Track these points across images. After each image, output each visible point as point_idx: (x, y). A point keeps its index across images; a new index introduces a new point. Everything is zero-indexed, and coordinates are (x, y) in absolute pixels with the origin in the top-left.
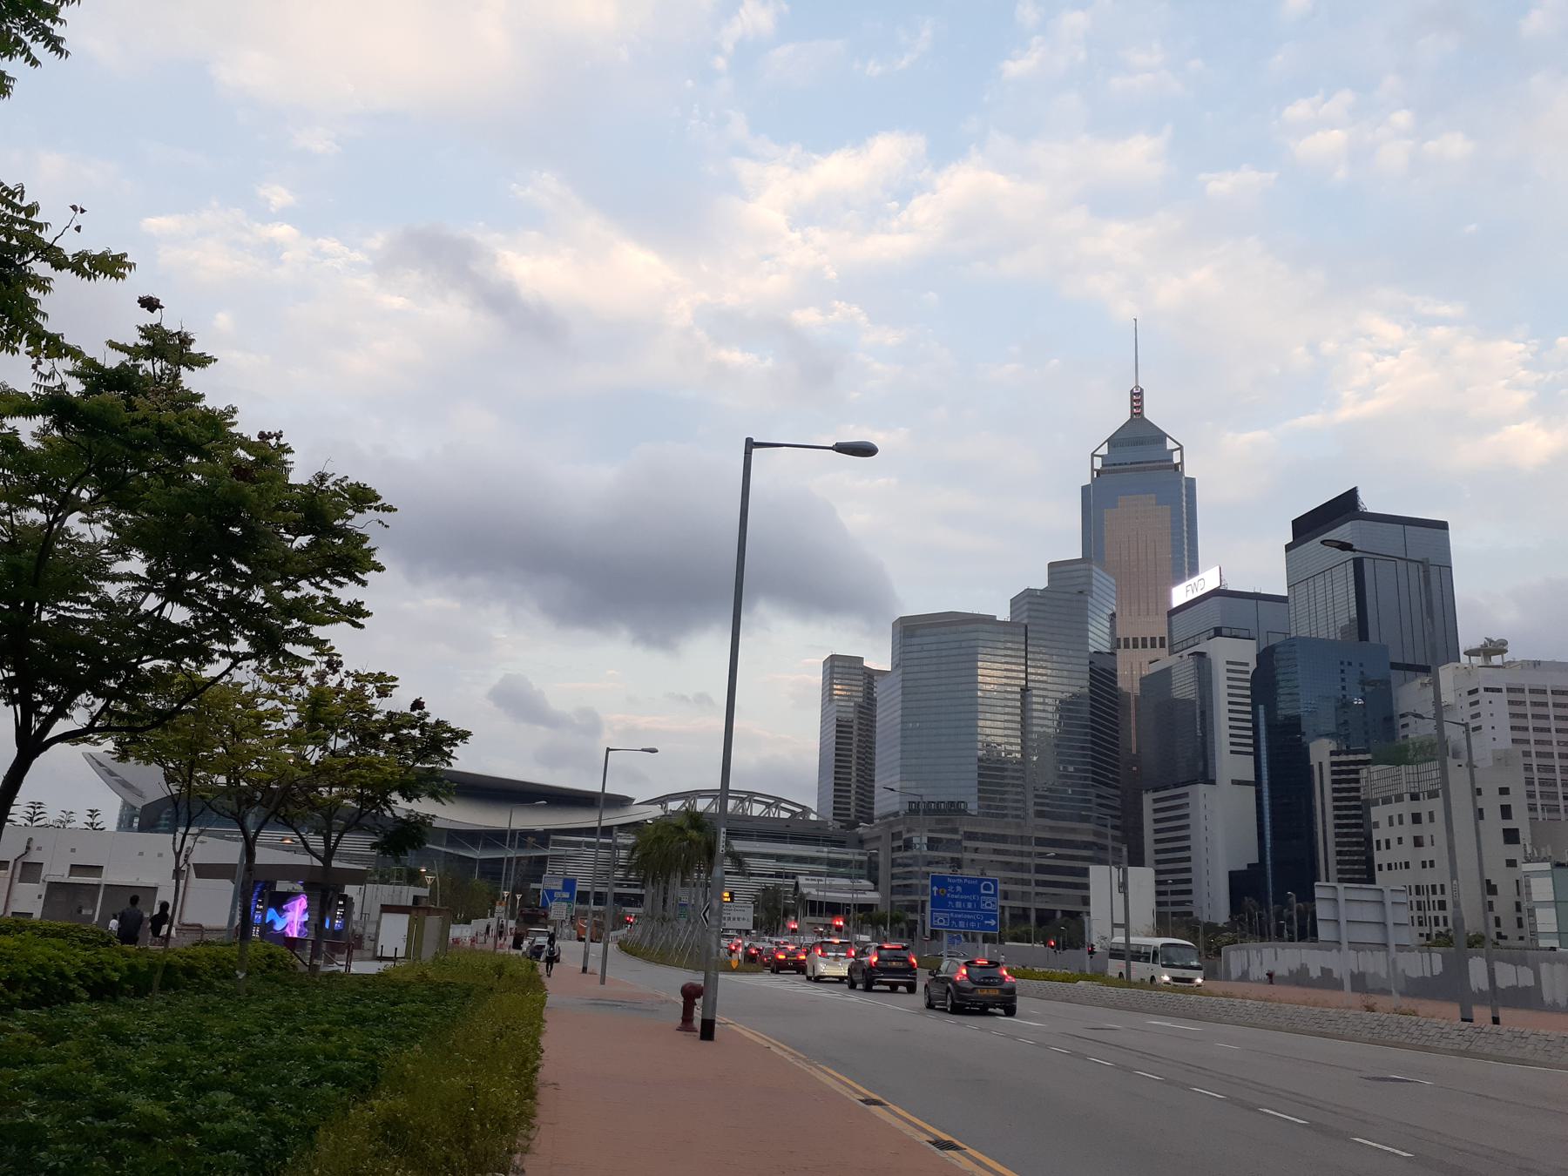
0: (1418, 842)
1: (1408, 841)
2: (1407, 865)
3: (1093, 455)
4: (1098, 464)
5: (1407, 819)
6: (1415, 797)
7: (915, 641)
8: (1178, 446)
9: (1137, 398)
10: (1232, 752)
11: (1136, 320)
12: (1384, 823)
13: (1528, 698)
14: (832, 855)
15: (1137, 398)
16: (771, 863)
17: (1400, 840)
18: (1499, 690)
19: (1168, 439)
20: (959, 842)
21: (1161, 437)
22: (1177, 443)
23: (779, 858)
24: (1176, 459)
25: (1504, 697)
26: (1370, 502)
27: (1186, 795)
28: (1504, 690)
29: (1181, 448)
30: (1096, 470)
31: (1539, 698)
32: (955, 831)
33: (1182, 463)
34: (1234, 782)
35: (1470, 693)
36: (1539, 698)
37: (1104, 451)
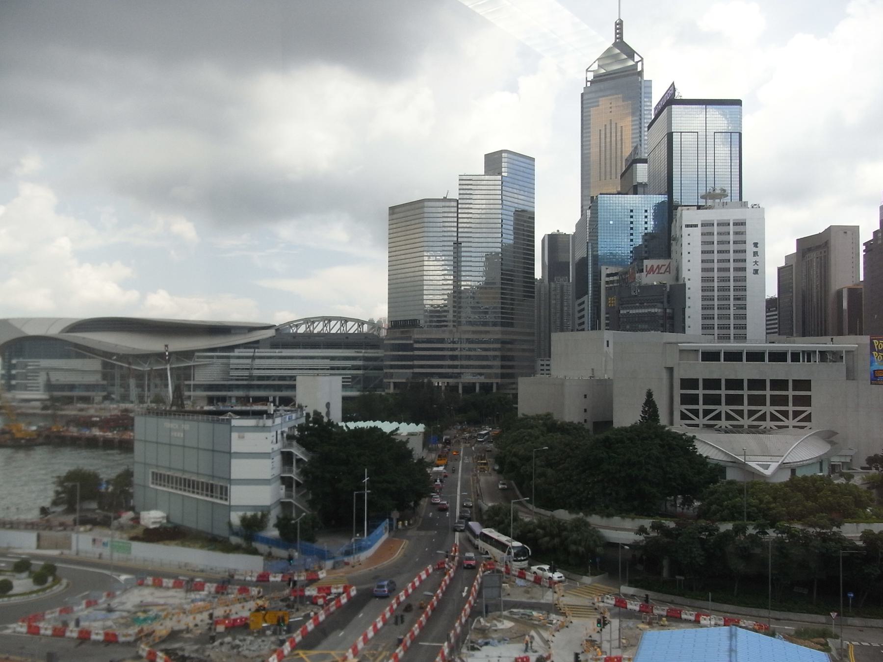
3: (587, 71)
8: (640, 59)
14: (366, 355)
16: (327, 362)
18: (696, 226)
19: (635, 54)
23: (333, 358)
25: (698, 231)
26: (683, 93)
28: (700, 226)
29: (642, 60)
30: (589, 81)
32: (409, 338)
36: (724, 229)
37: (595, 67)
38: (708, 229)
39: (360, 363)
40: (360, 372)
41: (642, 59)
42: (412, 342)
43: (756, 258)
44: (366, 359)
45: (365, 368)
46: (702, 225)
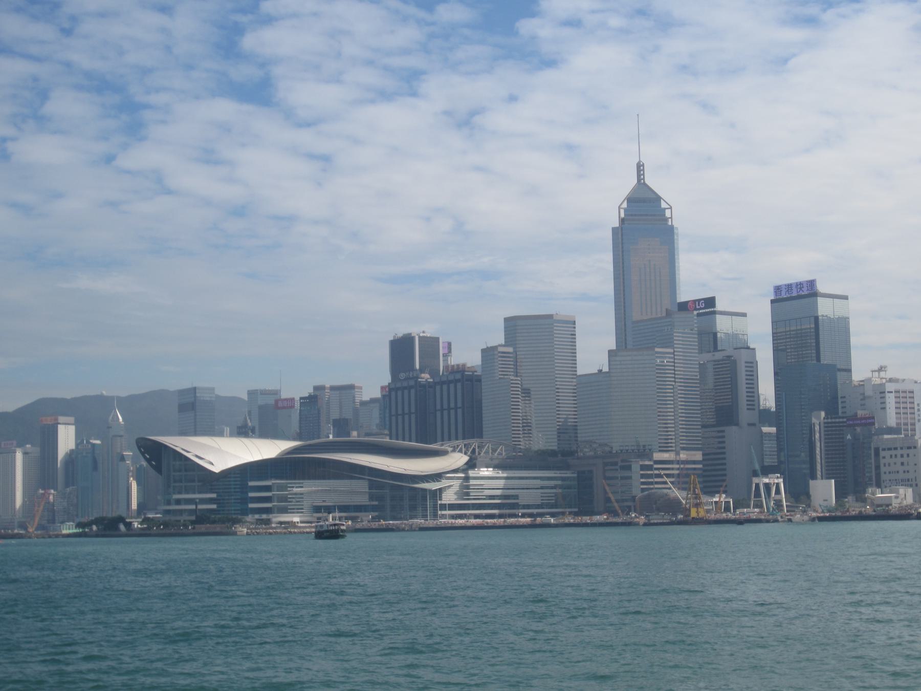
0: (902, 464)
1: (899, 464)
2: (898, 472)
3: (619, 208)
4: (622, 215)
5: (899, 456)
6: (902, 448)
7: (618, 358)
9: (640, 168)
10: (748, 409)
11: (638, 115)
13: (901, 395)
14: (563, 475)
15: (640, 168)
17: (895, 463)
18: (892, 392)
19: (662, 200)
20: (652, 466)
21: (658, 199)
22: (669, 205)
25: (892, 395)
27: (723, 431)
29: (671, 208)
31: (904, 395)
33: (671, 218)
34: (750, 425)
35: (881, 393)
36: (904, 395)
37: (625, 205)
38: (898, 395)
39: (559, 482)
40: (560, 491)
41: (671, 207)
42: (651, 463)
43: (919, 413)
44: (563, 479)
45: (561, 487)
46: (895, 392)
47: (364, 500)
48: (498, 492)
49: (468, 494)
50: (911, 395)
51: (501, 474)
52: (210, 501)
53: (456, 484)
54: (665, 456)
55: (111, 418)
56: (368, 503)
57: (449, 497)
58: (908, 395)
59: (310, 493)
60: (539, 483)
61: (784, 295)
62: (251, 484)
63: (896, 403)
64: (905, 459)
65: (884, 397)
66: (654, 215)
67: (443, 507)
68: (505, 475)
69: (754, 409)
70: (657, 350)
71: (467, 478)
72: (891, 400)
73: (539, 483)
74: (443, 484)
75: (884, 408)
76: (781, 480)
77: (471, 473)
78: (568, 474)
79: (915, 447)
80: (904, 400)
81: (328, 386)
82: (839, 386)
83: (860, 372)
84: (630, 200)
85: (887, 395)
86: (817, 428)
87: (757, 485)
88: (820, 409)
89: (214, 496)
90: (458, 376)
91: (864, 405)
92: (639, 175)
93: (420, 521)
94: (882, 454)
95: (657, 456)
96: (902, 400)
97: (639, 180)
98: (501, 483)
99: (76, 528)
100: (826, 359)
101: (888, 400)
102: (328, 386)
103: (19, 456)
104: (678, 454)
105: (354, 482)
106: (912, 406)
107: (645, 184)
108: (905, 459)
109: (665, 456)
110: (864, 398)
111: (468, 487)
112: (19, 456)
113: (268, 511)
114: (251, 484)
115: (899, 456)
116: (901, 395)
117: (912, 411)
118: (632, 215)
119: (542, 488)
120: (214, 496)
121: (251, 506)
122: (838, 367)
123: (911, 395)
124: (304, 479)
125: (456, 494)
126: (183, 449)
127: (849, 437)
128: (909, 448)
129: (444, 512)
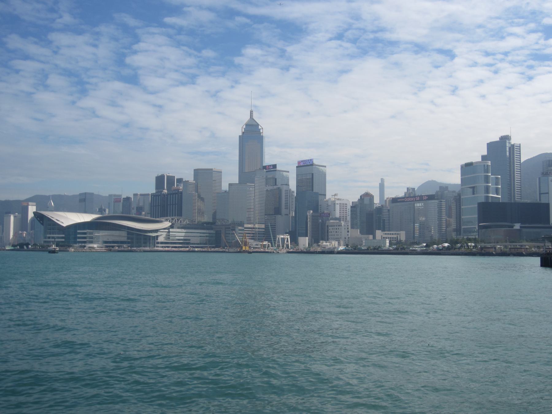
0: (336, 232)
1: (335, 232)
4: (243, 131)
5: (335, 229)
6: (336, 226)
12: (331, 229)
13: (342, 205)
19: (259, 126)
21: (258, 125)
24: (261, 131)
25: (338, 205)
29: (263, 129)
31: (343, 205)
36: (343, 205)
37: (244, 127)
38: (340, 205)
39: (208, 235)
40: (208, 238)
42: (244, 228)
44: (209, 233)
47: (125, 239)
48: (182, 238)
49: (169, 238)
50: (346, 205)
51: (183, 230)
52: (62, 238)
53: (164, 234)
54: (250, 226)
55: (48, 204)
56: (126, 240)
57: (161, 239)
58: (345, 205)
59: (102, 236)
60: (199, 235)
61: (302, 164)
62: (78, 231)
63: (340, 208)
64: (337, 230)
65: (335, 206)
66: (256, 131)
67: (158, 243)
68: (185, 231)
69: (287, 209)
70: (248, 184)
71: (169, 232)
72: (338, 207)
73: (199, 235)
74: (159, 234)
75: (335, 210)
76: (289, 237)
77: (171, 230)
78: (212, 232)
79: (341, 226)
80: (343, 207)
81: (139, 194)
82: (319, 201)
83: (329, 196)
84: (247, 125)
85: (336, 205)
86: (309, 217)
87: (279, 238)
88: (310, 210)
89: (64, 236)
90: (177, 192)
91: (328, 208)
92: (251, 115)
93: (147, 249)
94: (330, 228)
95: (246, 226)
96: (342, 207)
97: (251, 117)
98: (183, 234)
99: (12, 247)
100: (316, 190)
101: (336, 207)
102: (139, 194)
103: (12, 218)
104: (255, 225)
105: (121, 232)
106: (346, 209)
107: (253, 119)
108: (337, 230)
109: (250, 226)
110: (328, 206)
111: (169, 235)
112: (12, 218)
113: (85, 242)
114: (78, 231)
115: (335, 229)
116: (342, 205)
117: (346, 212)
118: (247, 131)
119: (200, 237)
120: (64, 236)
121: (78, 240)
122: (319, 193)
123: (346, 205)
124: (100, 230)
125: (164, 238)
126: (51, 217)
127: (320, 221)
128: (339, 226)
129: (158, 245)
